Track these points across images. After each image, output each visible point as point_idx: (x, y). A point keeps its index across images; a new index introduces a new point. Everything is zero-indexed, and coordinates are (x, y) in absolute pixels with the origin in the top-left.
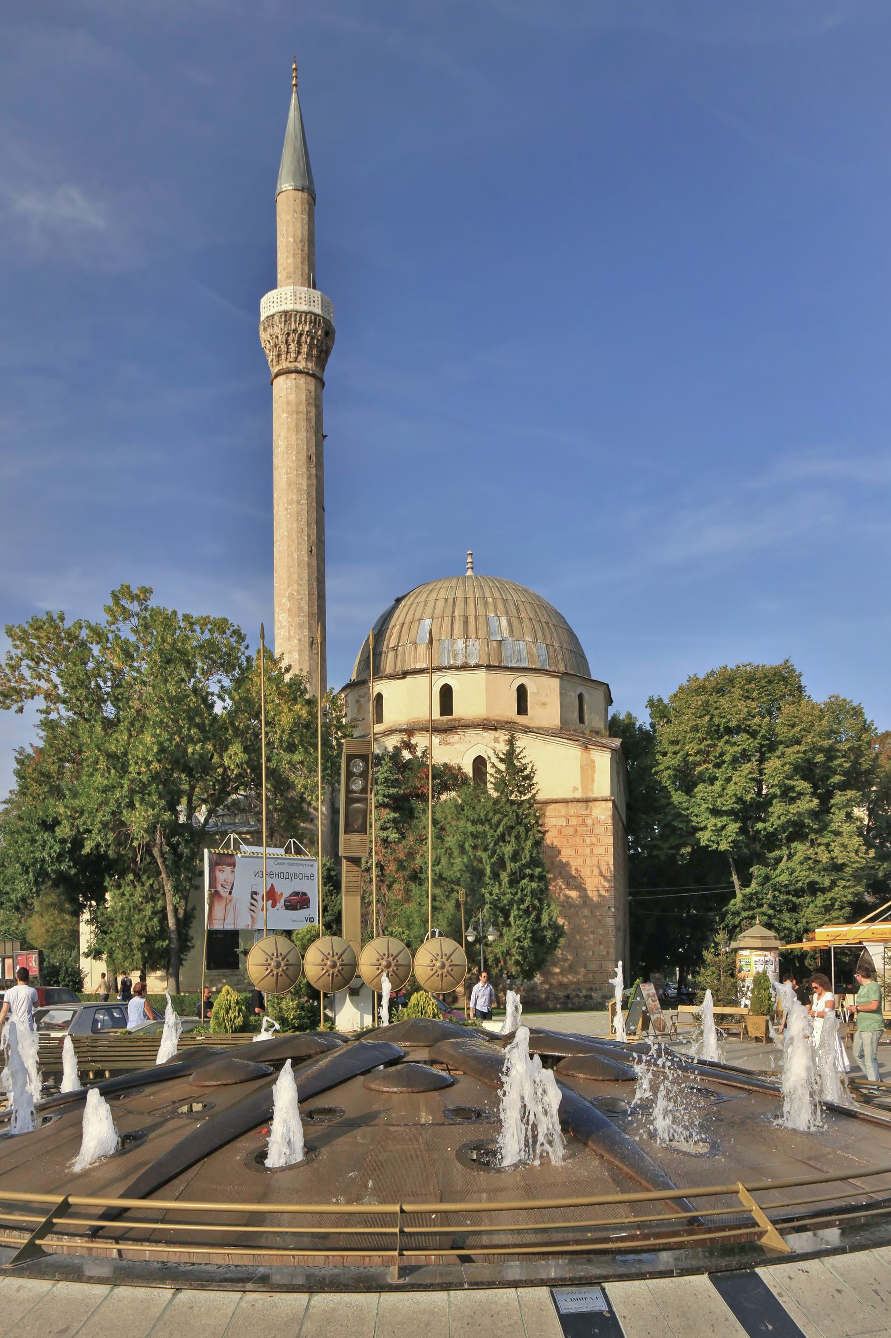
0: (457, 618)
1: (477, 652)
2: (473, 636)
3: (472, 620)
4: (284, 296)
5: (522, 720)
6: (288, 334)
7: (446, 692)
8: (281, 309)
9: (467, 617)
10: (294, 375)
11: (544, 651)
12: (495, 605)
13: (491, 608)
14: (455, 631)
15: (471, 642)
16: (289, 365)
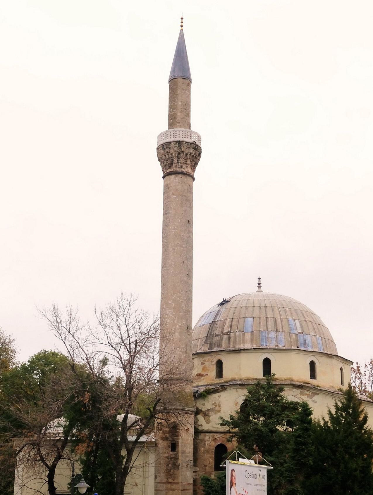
0: (270, 319)
1: (283, 339)
2: (281, 330)
3: (279, 321)
4: (178, 133)
5: (314, 382)
6: (179, 154)
7: (267, 363)
8: (177, 139)
9: (275, 318)
10: (180, 176)
11: (320, 342)
12: (291, 313)
13: (289, 314)
14: (269, 327)
15: (279, 333)
16: (178, 170)
